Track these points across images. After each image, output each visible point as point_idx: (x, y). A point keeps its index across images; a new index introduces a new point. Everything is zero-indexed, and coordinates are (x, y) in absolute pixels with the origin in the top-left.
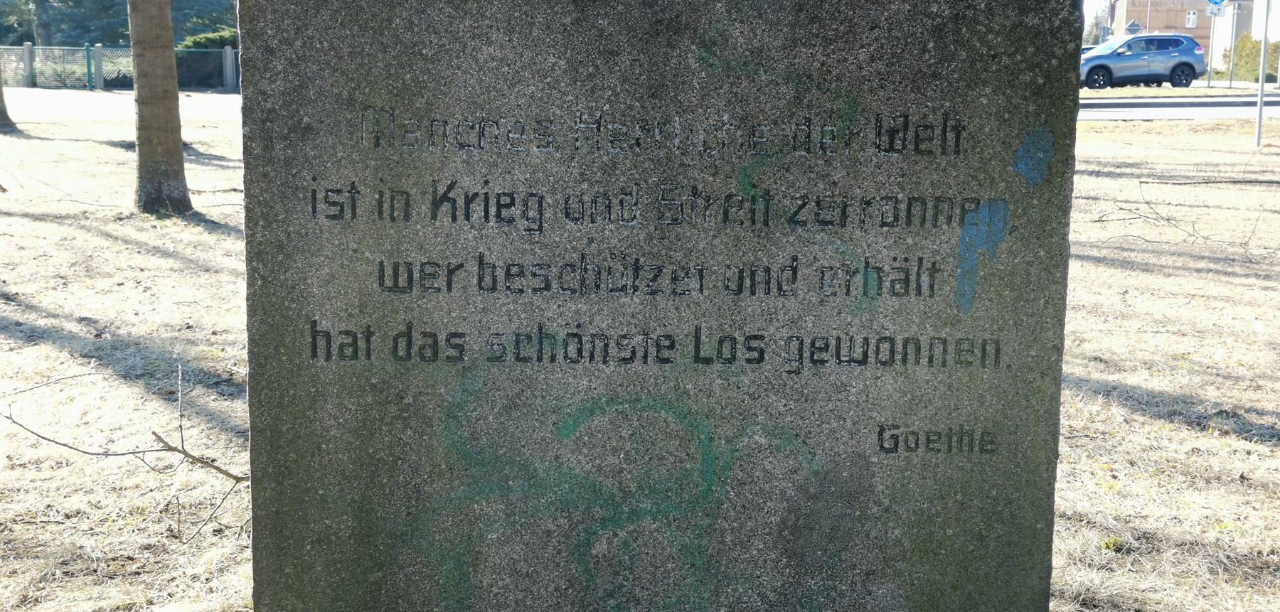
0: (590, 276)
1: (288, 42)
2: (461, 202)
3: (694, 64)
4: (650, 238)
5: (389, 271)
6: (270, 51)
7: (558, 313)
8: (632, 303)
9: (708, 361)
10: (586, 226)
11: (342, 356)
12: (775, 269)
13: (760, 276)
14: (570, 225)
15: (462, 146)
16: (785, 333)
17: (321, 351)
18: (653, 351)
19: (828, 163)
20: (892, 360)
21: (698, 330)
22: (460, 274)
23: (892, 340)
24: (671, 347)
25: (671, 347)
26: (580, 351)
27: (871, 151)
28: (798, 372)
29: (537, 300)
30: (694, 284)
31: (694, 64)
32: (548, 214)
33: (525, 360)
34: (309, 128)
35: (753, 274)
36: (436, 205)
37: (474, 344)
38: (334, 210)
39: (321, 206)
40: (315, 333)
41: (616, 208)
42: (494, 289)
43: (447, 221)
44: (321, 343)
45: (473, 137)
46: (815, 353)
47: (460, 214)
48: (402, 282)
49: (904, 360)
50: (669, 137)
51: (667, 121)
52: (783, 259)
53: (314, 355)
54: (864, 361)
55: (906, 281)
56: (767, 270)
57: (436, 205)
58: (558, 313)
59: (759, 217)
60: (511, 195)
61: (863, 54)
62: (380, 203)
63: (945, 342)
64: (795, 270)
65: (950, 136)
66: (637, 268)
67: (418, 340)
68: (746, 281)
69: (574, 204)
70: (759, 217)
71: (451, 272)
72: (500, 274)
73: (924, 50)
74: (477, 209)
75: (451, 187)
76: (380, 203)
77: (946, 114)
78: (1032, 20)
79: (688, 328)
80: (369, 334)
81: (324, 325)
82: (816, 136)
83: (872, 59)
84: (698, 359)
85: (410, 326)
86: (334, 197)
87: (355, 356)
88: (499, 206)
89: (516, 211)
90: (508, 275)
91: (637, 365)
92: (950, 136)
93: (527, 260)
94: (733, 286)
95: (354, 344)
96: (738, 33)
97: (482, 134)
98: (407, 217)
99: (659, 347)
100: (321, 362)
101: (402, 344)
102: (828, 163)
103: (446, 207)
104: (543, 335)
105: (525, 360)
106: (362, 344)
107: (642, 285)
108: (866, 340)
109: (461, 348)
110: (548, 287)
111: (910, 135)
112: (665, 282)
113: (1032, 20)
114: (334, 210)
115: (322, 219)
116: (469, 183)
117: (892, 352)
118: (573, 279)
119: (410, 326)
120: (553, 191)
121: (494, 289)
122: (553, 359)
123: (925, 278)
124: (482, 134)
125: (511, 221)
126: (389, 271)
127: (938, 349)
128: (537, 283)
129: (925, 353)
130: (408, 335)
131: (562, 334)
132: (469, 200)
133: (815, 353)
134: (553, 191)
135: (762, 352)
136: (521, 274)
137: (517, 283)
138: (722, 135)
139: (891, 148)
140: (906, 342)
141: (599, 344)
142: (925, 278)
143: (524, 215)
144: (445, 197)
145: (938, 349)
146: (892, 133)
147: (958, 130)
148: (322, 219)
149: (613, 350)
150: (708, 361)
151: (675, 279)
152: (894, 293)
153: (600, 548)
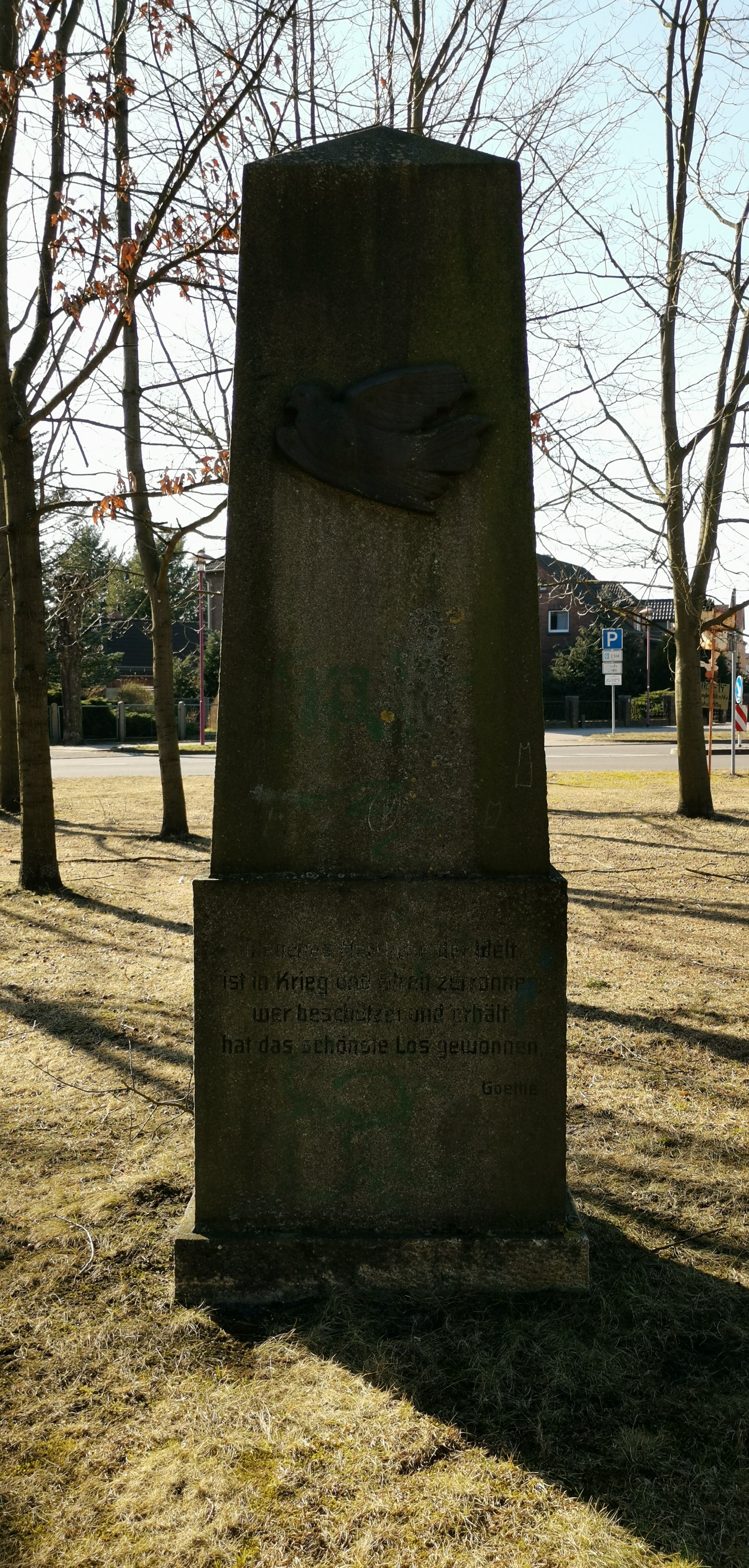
0: (349, 1014)
1: (215, 912)
2: (290, 981)
3: (394, 919)
4: (375, 996)
5: (258, 1012)
6: (206, 916)
7: (334, 1031)
9: (403, 1052)
10: (347, 991)
11: (236, 1051)
12: (433, 1009)
13: (426, 1013)
14: (339, 991)
15: (291, 956)
16: (438, 1039)
17: (227, 1050)
18: (378, 1048)
19: (455, 962)
20: (487, 1052)
21: (398, 1038)
22: (290, 1014)
23: (487, 1042)
24: (386, 1046)
25: (386, 1046)
26: (344, 1048)
27: (474, 957)
28: (444, 1057)
29: (325, 1025)
30: (396, 1017)
31: (394, 919)
32: (329, 986)
33: (320, 1052)
34: (223, 949)
35: (423, 1013)
37: (296, 1045)
38: (233, 985)
39: (228, 984)
40: (224, 1041)
41: (360, 983)
42: (305, 1020)
43: (284, 989)
44: (227, 1045)
45: (296, 952)
46: (453, 1048)
47: (290, 986)
49: (493, 1051)
50: (384, 951)
51: (383, 944)
52: (436, 1005)
53: (224, 1051)
54: (474, 1052)
55: (492, 1015)
56: (429, 1011)
58: (334, 1031)
59: (425, 986)
61: (469, 914)
62: (254, 982)
63: (511, 1043)
64: (442, 1011)
65: (510, 950)
66: (370, 1010)
67: (271, 1044)
68: (419, 1016)
69: (341, 981)
70: (425, 986)
71: (286, 1013)
72: (308, 1013)
73: (496, 912)
74: (298, 985)
75: (286, 974)
76: (254, 982)
77: (507, 941)
78: (544, 899)
79: (393, 1038)
80: (248, 1041)
81: (229, 1037)
82: (449, 950)
83: (473, 916)
84: (398, 1051)
85: (267, 1037)
86: (234, 980)
87: (242, 1051)
88: (308, 983)
89: (315, 985)
90: (312, 1014)
91: (370, 1055)
92: (510, 950)
93: (320, 1007)
94: (414, 1018)
95: (242, 1046)
96: (413, 905)
97: (300, 951)
98: (266, 988)
99: (380, 1046)
101: (264, 1045)
102: (455, 962)
103: (284, 983)
104: (328, 1041)
105: (320, 1052)
106: (245, 1046)
107: (373, 1019)
108: (475, 1043)
109: (290, 1047)
110: (329, 1019)
111: (492, 950)
112: (383, 1016)
113: (544, 899)
114: (233, 985)
115: (228, 989)
116: (293, 972)
117: (487, 1047)
118: (341, 1015)
119: (267, 1037)
120: (332, 976)
121: (305, 1020)
122: (332, 1052)
123: (501, 1013)
124: (300, 951)
125: (312, 989)
126: (258, 1012)
127: (508, 1046)
128: (325, 1017)
129: (502, 1048)
130: (266, 1041)
131: (336, 1040)
132: (294, 980)
133: (453, 1048)
134: (332, 976)
135: (428, 1048)
136: (317, 1013)
138: (407, 950)
139: (483, 955)
140: (494, 1043)
141: (353, 1045)
142: (501, 1013)
143: (319, 987)
144: (283, 979)
145: (508, 1046)
146: (484, 948)
147: (513, 947)
148: (228, 989)
149: (359, 1048)
150: (403, 1052)
151: (387, 1015)
152: (487, 1021)
153: (355, 1140)
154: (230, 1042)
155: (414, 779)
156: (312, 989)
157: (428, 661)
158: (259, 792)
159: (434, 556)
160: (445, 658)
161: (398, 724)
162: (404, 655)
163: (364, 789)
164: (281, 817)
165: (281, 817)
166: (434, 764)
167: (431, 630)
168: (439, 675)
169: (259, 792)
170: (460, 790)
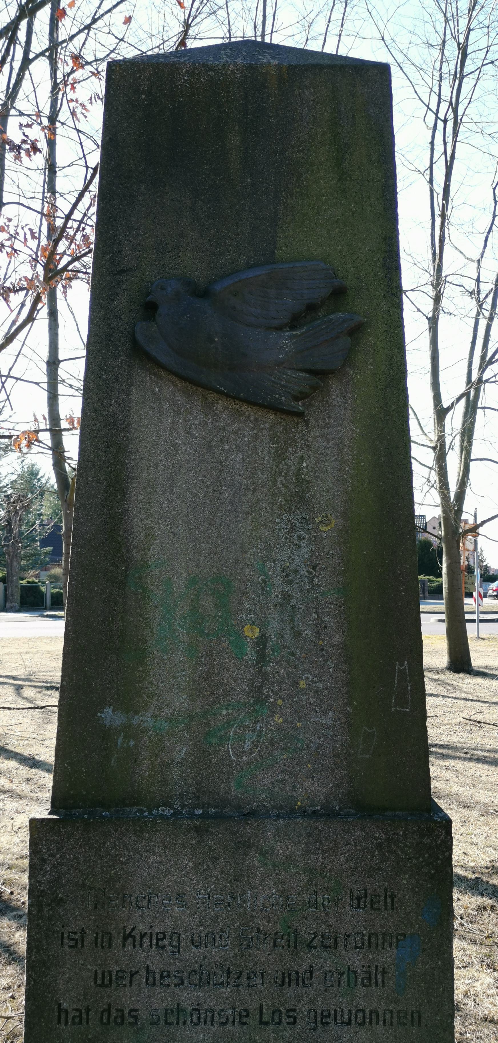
0: (205, 977)
1: (53, 856)
2: (138, 938)
3: (257, 864)
4: (236, 956)
5: (100, 976)
6: (44, 860)
7: (187, 997)
8: (227, 991)
9: (267, 1024)
10: (202, 950)
11: (73, 1023)
12: (301, 971)
13: (293, 976)
14: (194, 949)
15: (139, 908)
16: (307, 1007)
17: (63, 1020)
18: (237, 1018)
19: (327, 914)
20: (364, 1023)
21: (261, 1006)
22: (137, 977)
23: (363, 1011)
24: (247, 1016)
25: (247, 1016)
26: (199, 1018)
27: (348, 908)
28: (314, 1029)
29: (177, 991)
30: (259, 981)
31: (257, 864)
32: (183, 943)
33: (170, 1024)
34: (61, 899)
35: (290, 975)
36: (125, 939)
37: (143, 1015)
38: (72, 943)
39: (66, 941)
40: (60, 1010)
41: (218, 940)
42: (154, 984)
43: (130, 948)
44: (63, 1016)
45: (145, 903)
46: (324, 1018)
47: (137, 943)
48: (106, 981)
49: (371, 1023)
50: (245, 901)
51: (244, 893)
52: (305, 966)
53: (59, 1022)
54: (349, 1023)
55: (370, 978)
56: (297, 973)
57: (125, 939)
58: (187, 997)
59: (292, 944)
60: (164, 933)
61: (342, 858)
62: (96, 938)
63: (391, 1012)
64: (311, 973)
65: (389, 900)
66: (229, 972)
67: (114, 1014)
68: (285, 979)
69: (196, 938)
70: (292, 944)
71: (132, 975)
72: (158, 976)
73: (373, 856)
75: (133, 929)
76: (96, 938)
77: (386, 890)
78: (427, 841)
79: (255, 1005)
80: (88, 1010)
81: (65, 1005)
82: (320, 900)
83: (347, 861)
84: (261, 1022)
85: (109, 1006)
86: (73, 936)
87: (80, 1023)
88: (158, 940)
89: (166, 942)
90: (162, 977)
91: (229, 1027)
92: (389, 900)
93: (172, 968)
94: (279, 981)
95: (80, 1016)
96: (278, 847)
97: (149, 901)
98: (110, 946)
99: (241, 1016)
100: (63, 1026)
101: (105, 1015)
102: (327, 914)
103: (130, 940)
104: (180, 1009)
105: (170, 1024)
106: (84, 1016)
107: (232, 981)
108: (350, 1011)
109: (136, 1018)
110: (182, 983)
111: (368, 900)
112: (244, 980)
113: (427, 841)
114: (72, 943)
115: (66, 948)
116: (141, 927)
117: (364, 1017)
118: (195, 978)
119: (109, 1006)
120: (186, 931)
121: (154, 984)
122: (185, 1023)
123: (379, 977)
124: (149, 901)
125: (163, 947)
126: (100, 976)
127: (388, 1016)
128: (177, 981)
129: (381, 1018)
130: (109, 1011)
131: (190, 1009)
132: (142, 936)
133: (324, 1018)
134: (186, 931)
135: (295, 1018)
136: (169, 976)
137: (167, 981)
138: (272, 900)
139: (359, 907)
140: (371, 1012)
141: (209, 1014)
142: (379, 977)
143: (170, 944)
144: (130, 935)
145: (388, 1016)
146: (359, 899)
147: (393, 897)
148: (66, 948)
149: (216, 1018)
150: (267, 1024)
151: (249, 978)
152: (363, 985)
154: (67, 1012)
155: (280, 702)
156: (163, 947)
157: (296, 571)
158: (110, 716)
159: (302, 458)
160: (314, 568)
161: (263, 640)
162: (270, 564)
163: (224, 712)
164: (132, 743)
165: (132, 743)
166: (302, 684)
167: (299, 538)
168: (308, 586)
169: (110, 716)
170: (331, 714)
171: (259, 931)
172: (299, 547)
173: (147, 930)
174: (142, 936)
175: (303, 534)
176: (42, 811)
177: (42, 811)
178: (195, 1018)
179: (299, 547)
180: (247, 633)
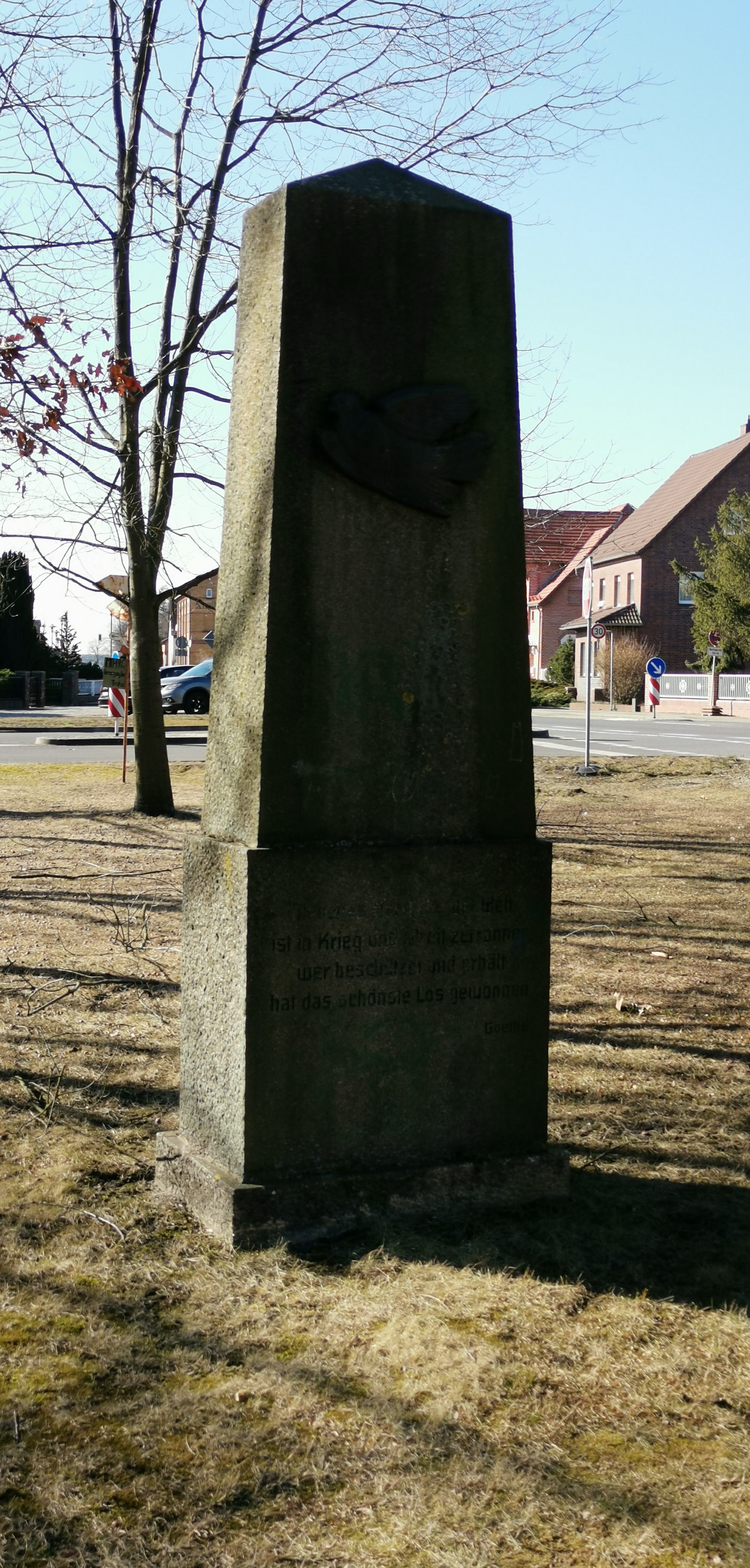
8: (394, 978)
15: (331, 918)
21: (418, 989)
36: (320, 943)
48: (307, 976)
54: (479, 997)
57: (320, 943)
60: (348, 937)
66: (396, 964)
67: (313, 1001)
72: (344, 970)
74: (336, 946)
80: (293, 999)
81: (276, 996)
89: (351, 944)
90: (348, 970)
91: (396, 1005)
100: (275, 1012)
103: (324, 944)
104: (361, 994)
109: (328, 1002)
125: (349, 948)
128: (358, 973)
132: (333, 940)
137: (351, 973)
144: (324, 940)
150: (422, 1001)
153: (381, 1084)
154: (278, 1001)
155: (429, 755)
156: (349, 948)
157: (441, 649)
158: (301, 767)
159: (445, 555)
160: (454, 646)
161: (416, 705)
162: (422, 642)
163: (388, 764)
164: (319, 789)
165: (319, 789)
166: (446, 741)
167: (444, 621)
168: (450, 661)
169: (301, 767)
170: (466, 765)
171: (417, 932)
172: (443, 628)
173: (337, 935)
174: (333, 940)
175: (447, 618)
176: (254, 846)
177: (254, 846)
178: (371, 1000)
179: (443, 628)
180: (405, 699)
